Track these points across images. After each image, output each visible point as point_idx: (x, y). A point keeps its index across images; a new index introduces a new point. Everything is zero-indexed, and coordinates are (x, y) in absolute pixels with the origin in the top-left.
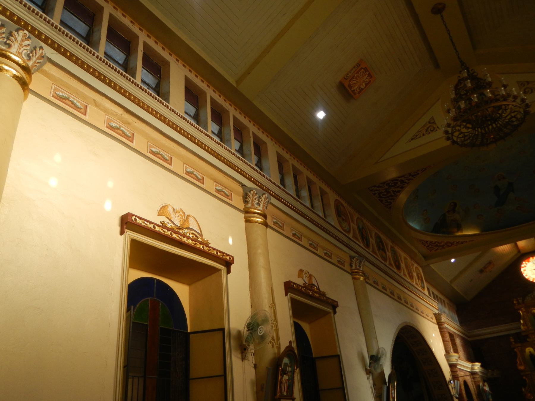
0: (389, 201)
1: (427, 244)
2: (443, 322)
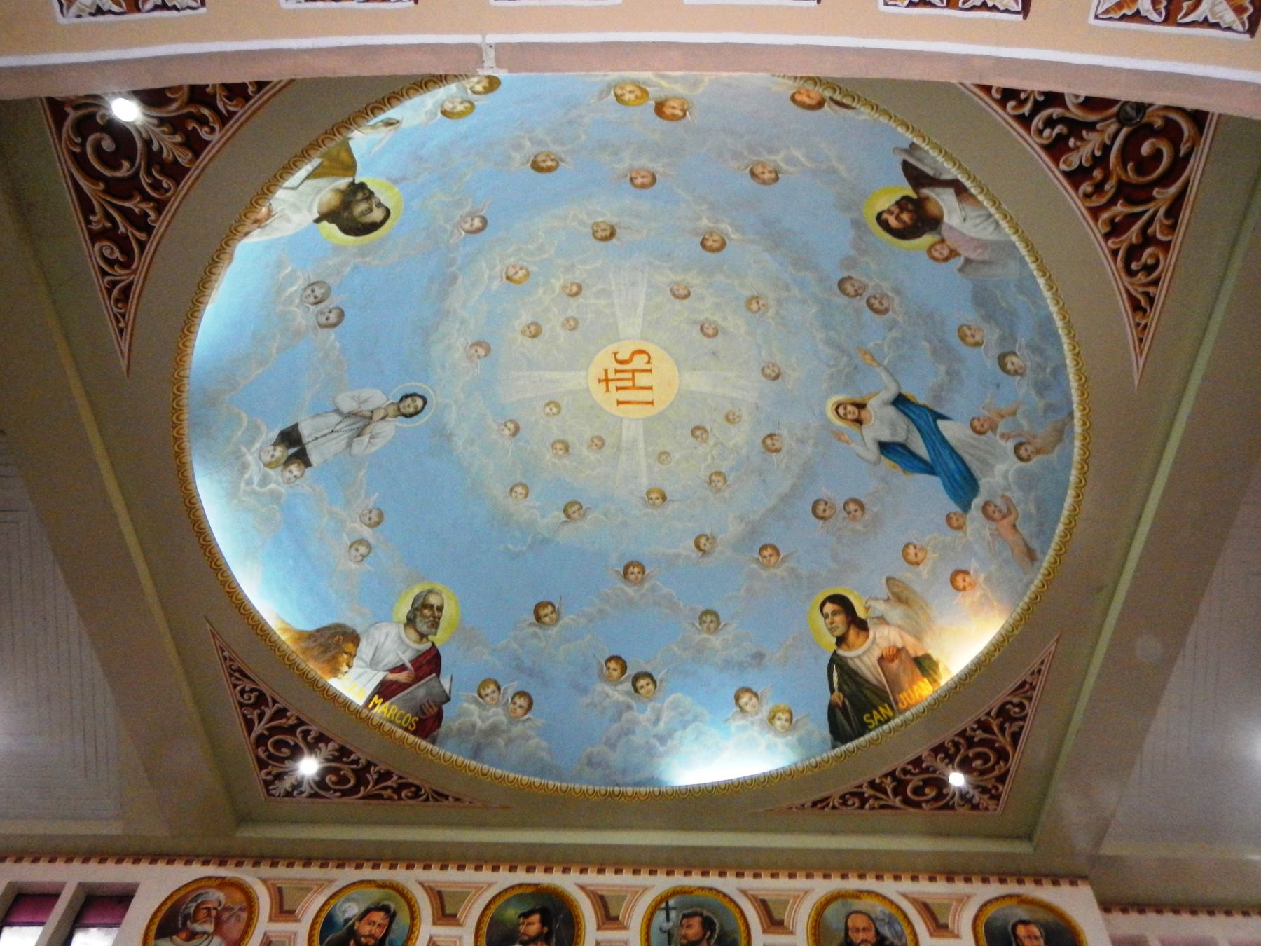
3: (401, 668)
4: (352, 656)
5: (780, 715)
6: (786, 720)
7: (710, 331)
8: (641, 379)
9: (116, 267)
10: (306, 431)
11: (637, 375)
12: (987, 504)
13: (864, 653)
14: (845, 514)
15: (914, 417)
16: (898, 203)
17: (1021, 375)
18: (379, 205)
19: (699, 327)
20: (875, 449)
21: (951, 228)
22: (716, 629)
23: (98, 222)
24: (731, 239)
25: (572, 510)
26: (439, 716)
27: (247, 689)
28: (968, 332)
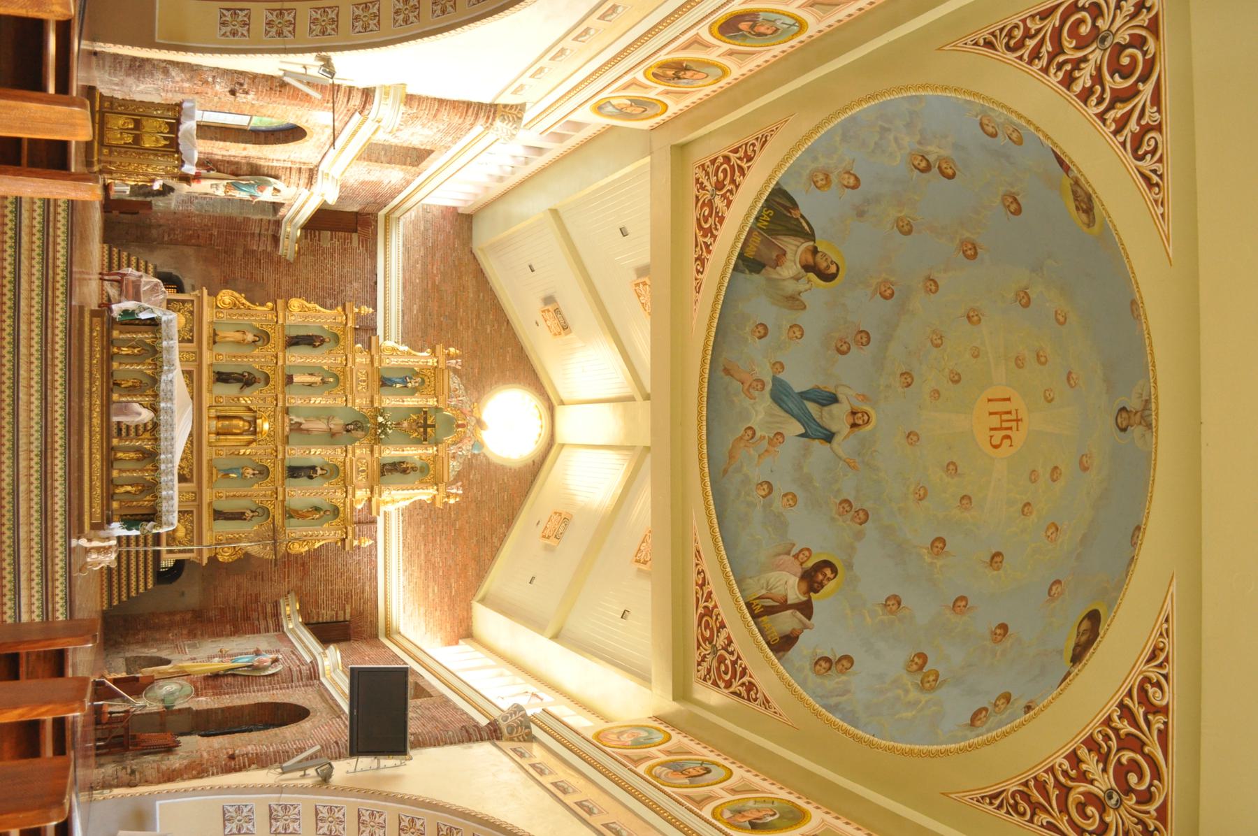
0: (1031, 43)
1: (740, 159)
2: (491, 124)
5: (824, 182)
6: (817, 181)
7: (951, 467)
8: (995, 421)
9: (1155, 681)
11: (999, 426)
12: (763, 389)
13: (796, 251)
14: (847, 340)
15: (819, 428)
16: (823, 587)
17: (758, 484)
19: (959, 471)
20: (840, 396)
21: (795, 575)
22: (897, 222)
23: (1158, 722)
24: (927, 548)
25: (1024, 299)
27: (1148, 157)
28: (791, 502)
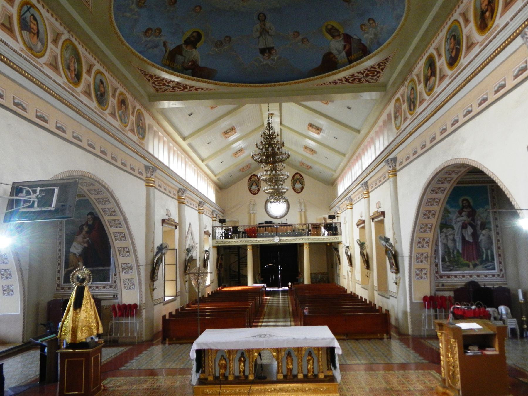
3: (345, 47)
4: (334, 56)
10: (262, 47)
18: (192, 34)
26: (364, 45)
